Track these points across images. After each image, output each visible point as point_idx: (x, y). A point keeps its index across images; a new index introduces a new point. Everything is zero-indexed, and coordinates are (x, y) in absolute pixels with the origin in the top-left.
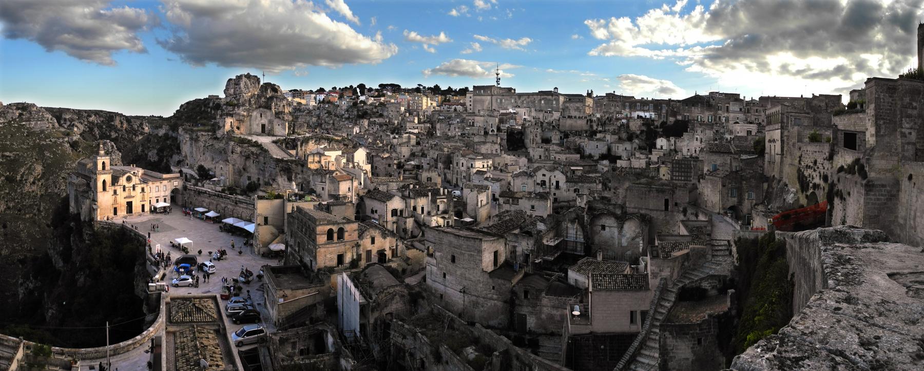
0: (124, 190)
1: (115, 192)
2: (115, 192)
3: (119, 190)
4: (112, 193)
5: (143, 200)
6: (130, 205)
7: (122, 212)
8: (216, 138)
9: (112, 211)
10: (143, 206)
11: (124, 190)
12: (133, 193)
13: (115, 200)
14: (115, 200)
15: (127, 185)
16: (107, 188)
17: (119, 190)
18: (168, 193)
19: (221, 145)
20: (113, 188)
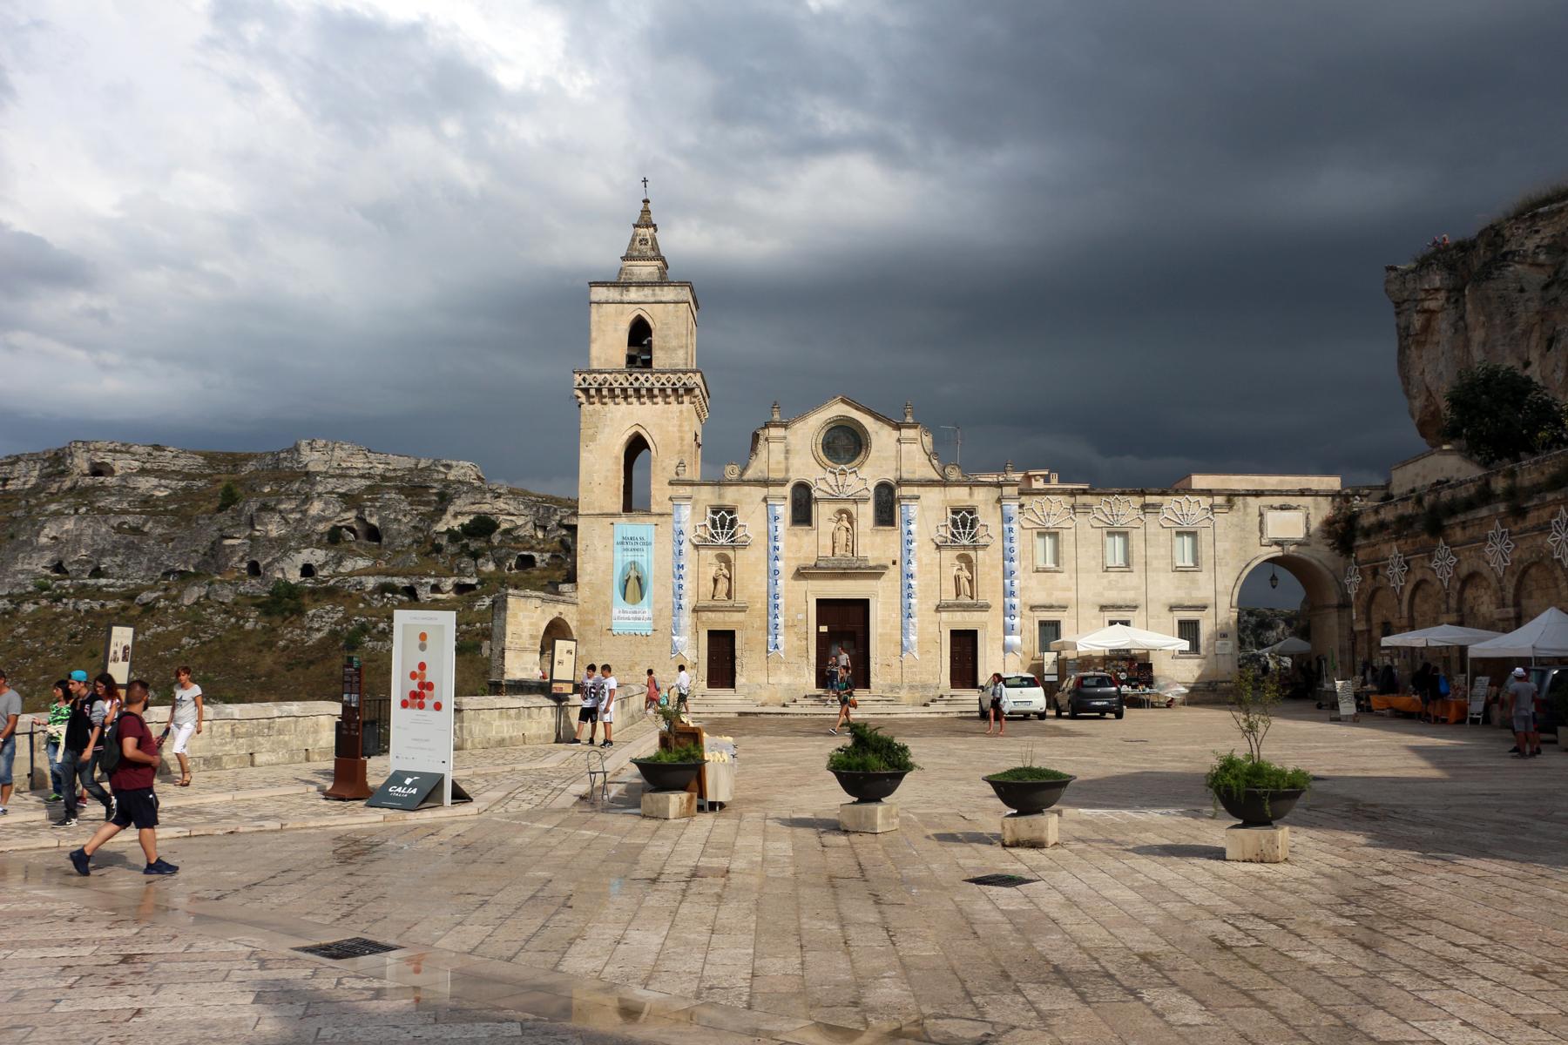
3: (758, 515)
5: (966, 596)
10: (964, 645)
12: (874, 544)
16: (660, 492)
17: (758, 515)
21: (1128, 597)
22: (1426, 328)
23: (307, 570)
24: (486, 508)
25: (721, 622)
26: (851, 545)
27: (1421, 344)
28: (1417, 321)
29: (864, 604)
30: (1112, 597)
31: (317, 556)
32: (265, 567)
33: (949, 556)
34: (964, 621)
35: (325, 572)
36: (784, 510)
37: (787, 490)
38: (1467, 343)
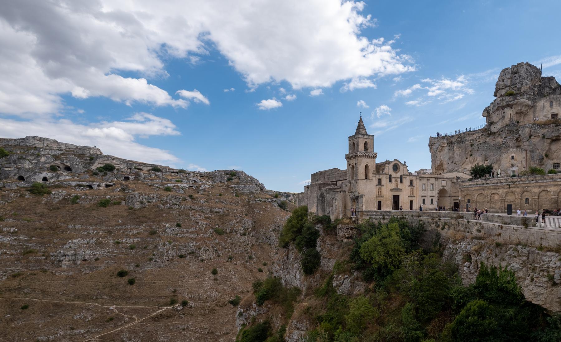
0: (390, 181)
1: (380, 182)
2: (380, 182)
3: (385, 181)
4: (375, 182)
6: (396, 199)
7: (387, 207)
8: (491, 134)
9: (376, 205)
11: (390, 181)
13: (380, 192)
14: (380, 192)
15: (394, 175)
16: (371, 175)
18: (435, 193)
19: (499, 140)
20: (377, 176)
21: (425, 195)
22: (442, 149)
23: (45, 179)
24: (109, 162)
25: (379, 199)
26: (397, 186)
27: (440, 152)
28: (440, 148)
29: (398, 196)
30: (423, 195)
31: (49, 175)
32: (27, 178)
33: (410, 188)
34: (411, 199)
35: (53, 180)
36: (388, 180)
37: (388, 176)
38: (453, 154)
